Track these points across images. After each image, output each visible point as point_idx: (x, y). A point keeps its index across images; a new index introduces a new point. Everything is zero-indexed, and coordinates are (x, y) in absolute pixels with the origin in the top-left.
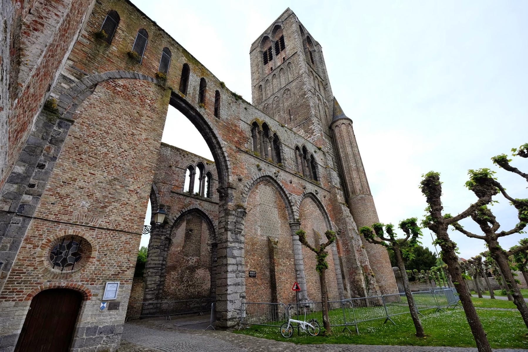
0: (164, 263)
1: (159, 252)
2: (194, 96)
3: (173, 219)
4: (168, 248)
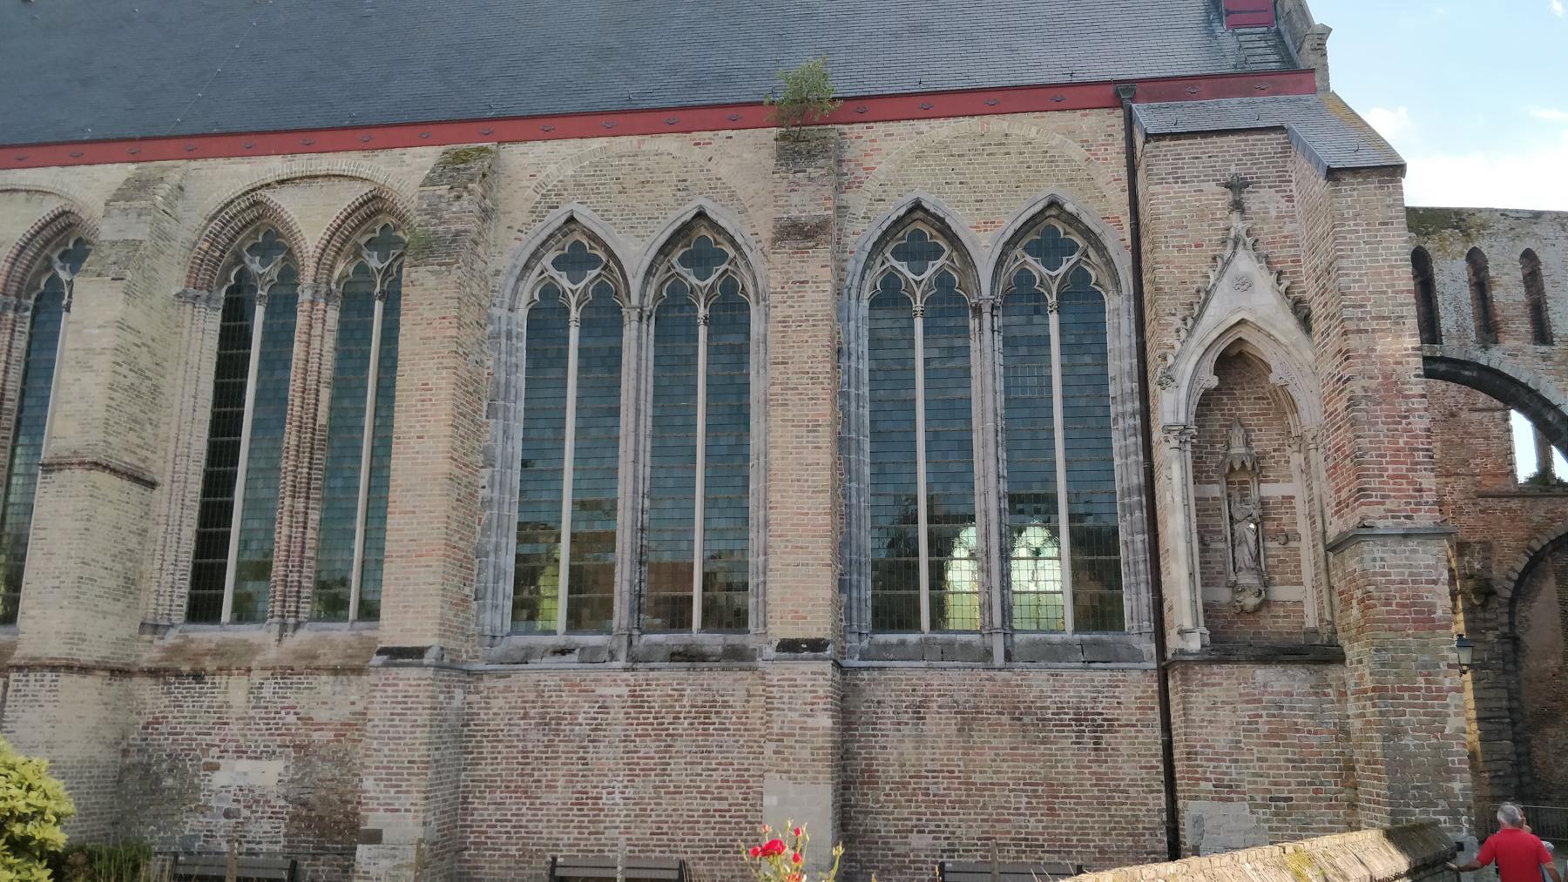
0: (1515, 704)
1: (1492, 677)
2: (1462, 329)
3: (1509, 578)
4: (1515, 662)
